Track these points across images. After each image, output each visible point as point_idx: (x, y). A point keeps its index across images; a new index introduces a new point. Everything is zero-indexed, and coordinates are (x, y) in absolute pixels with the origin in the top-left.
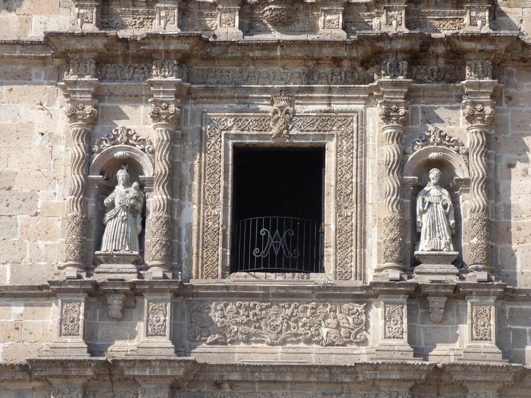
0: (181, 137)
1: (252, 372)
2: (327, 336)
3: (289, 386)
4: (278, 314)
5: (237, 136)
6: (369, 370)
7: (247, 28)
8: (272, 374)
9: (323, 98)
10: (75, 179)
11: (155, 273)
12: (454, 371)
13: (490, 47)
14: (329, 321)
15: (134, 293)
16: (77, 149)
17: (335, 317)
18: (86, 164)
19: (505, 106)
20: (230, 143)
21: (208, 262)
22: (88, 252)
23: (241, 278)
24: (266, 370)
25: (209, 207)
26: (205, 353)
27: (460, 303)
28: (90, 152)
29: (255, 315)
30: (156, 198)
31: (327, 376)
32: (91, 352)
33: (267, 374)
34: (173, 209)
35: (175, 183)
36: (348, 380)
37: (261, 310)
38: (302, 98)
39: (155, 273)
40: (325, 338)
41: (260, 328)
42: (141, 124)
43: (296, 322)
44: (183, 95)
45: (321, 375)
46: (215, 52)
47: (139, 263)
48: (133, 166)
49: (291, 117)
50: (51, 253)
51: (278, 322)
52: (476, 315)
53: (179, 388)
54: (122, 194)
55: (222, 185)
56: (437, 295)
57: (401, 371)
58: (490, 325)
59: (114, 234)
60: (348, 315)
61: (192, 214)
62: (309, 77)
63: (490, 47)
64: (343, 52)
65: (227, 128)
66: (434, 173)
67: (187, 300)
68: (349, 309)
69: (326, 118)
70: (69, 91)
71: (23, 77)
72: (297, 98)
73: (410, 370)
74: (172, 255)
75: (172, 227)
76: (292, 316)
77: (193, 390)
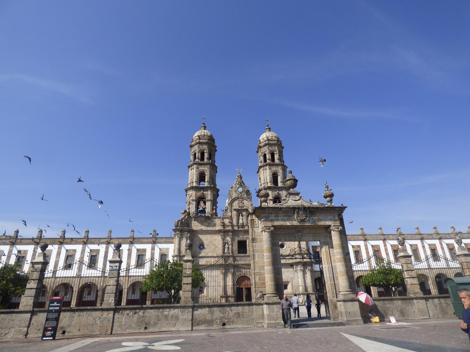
0: (233, 240)
4: (243, 258)
7: (238, 228)
10: (222, 245)
11: (231, 254)
15: (229, 257)
16: (222, 242)
18: (223, 243)
21: (236, 253)
22: (224, 253)
23: (239, 255)
25: (236, 247)
26: (236, 263)
30: (230, 246)
32: (225, 263)
34: (232, 247)
35: (232, 245)
39: (231, 254)
42: (228, 239)
44: (232, 235)
47: (229, 253)
48: (228, 244)
49: (243, 238)
50: (220, 252)
54: (227, 246)
55: (237, 245)
59: (226, 251)
61: (234, 248)
62: (245, 233)
65: (237, 239)
67: (234, 257)
69: (247, 237)
70: (221, 235)
71: (216, 234)
74: (232, 253)
75: (232, 249)
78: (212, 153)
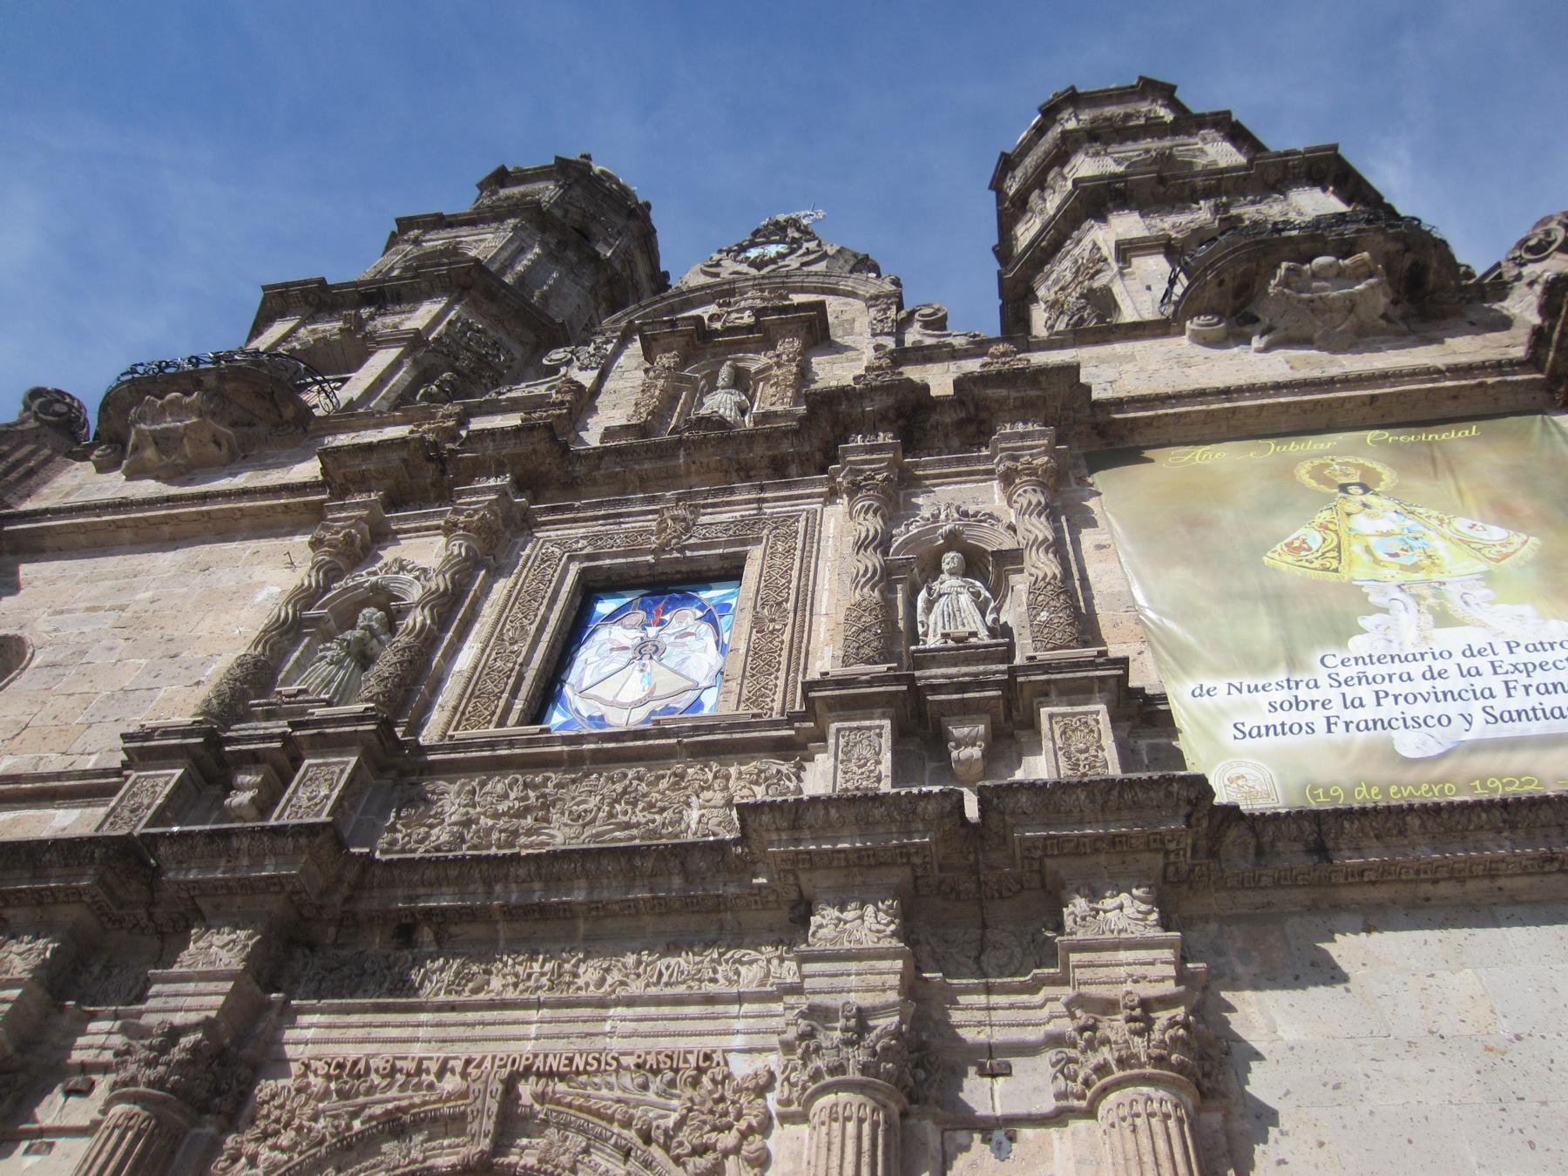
1: (488, 884)
2: (699, 822)
3: (582, 927)
5: (589, 557)
6: (778, 830)
8: (537, 885)
9: (749, 502)
12: (1013, 813)
13: (1033, 393)
14: (707, 795)
17: (726, 788)
19: (1075, 486)
20: (574, 568)
24: (522, 872)
27: (1024, 736)
28: (327, 589)
29: (544, 796)
31: (677, 881)
33: (525, 885)
36: (732, 889)
37: (559, 786)
38: (714, 505)
40: (693, 826)
41: (547, 820)
43: (634, 804)
45: (660, 880)
46: (580, 469)
51: (590, 806)
52: (1064, 733)
53: (312, 946)
56: (966, 711)
57: (865, 825)
58: (1101, 748)
60: (757, 783)
63: (1033, 393)
64: (787, 447)
66: (950, 559)
68: (761, 771)
72: (705, 506)
73: (893, 821)
76: (625, 792)
77: (345, 953)
78: (595, 228)
